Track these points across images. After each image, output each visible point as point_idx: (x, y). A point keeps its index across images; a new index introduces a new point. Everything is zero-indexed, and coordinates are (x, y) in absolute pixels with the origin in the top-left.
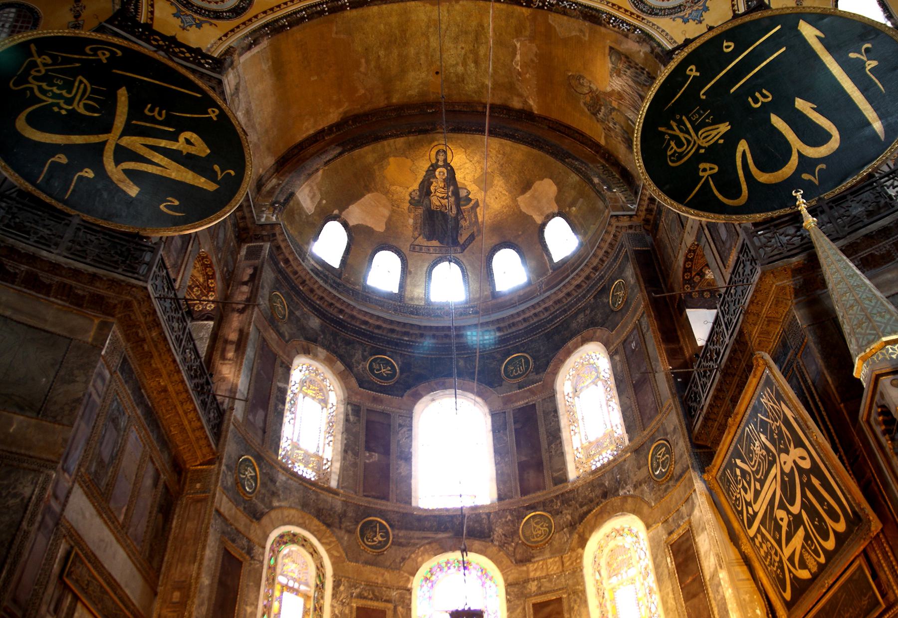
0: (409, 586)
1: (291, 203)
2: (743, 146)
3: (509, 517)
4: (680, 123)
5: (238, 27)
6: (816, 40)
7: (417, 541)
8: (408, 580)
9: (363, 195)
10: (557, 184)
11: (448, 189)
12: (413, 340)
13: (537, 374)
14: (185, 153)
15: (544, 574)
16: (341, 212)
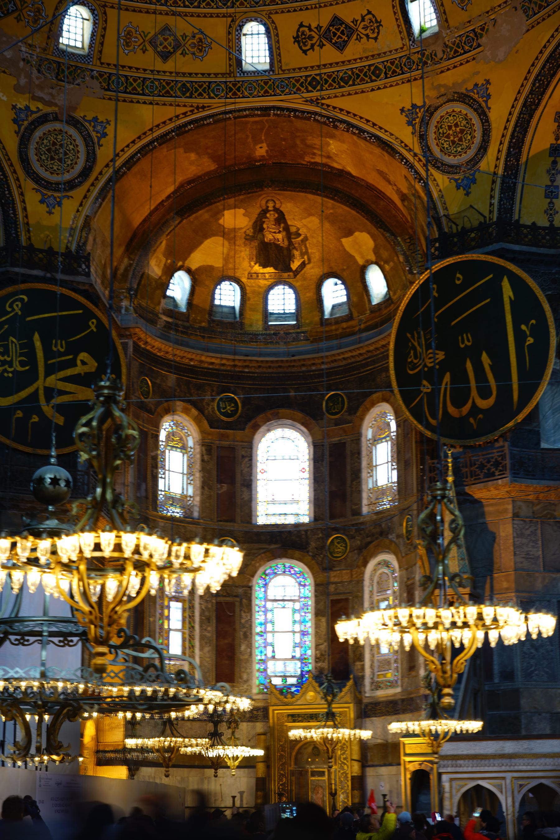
0: (250, 585)
1: (143, 282)
2: (447, 378)
3: (320, 535)
4: (419, 337)
5: (89, 191)
6: (508, 301)
7: (255, 551)
8: (250, 581)
9: (201, 243)
10: (374, 241)
11: (279, 225)
12: (253, 370)
13: (350, 414)
14: (83, 374)
15: (339, 581)
16: (184, 263)
